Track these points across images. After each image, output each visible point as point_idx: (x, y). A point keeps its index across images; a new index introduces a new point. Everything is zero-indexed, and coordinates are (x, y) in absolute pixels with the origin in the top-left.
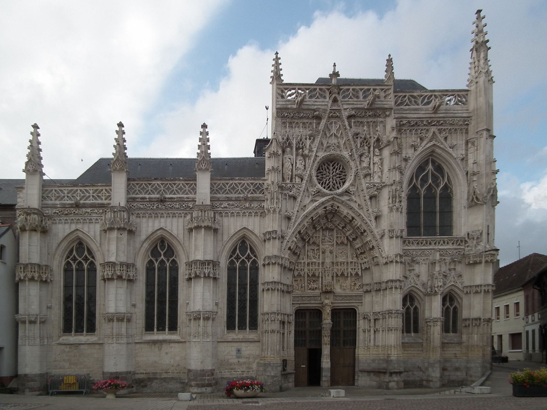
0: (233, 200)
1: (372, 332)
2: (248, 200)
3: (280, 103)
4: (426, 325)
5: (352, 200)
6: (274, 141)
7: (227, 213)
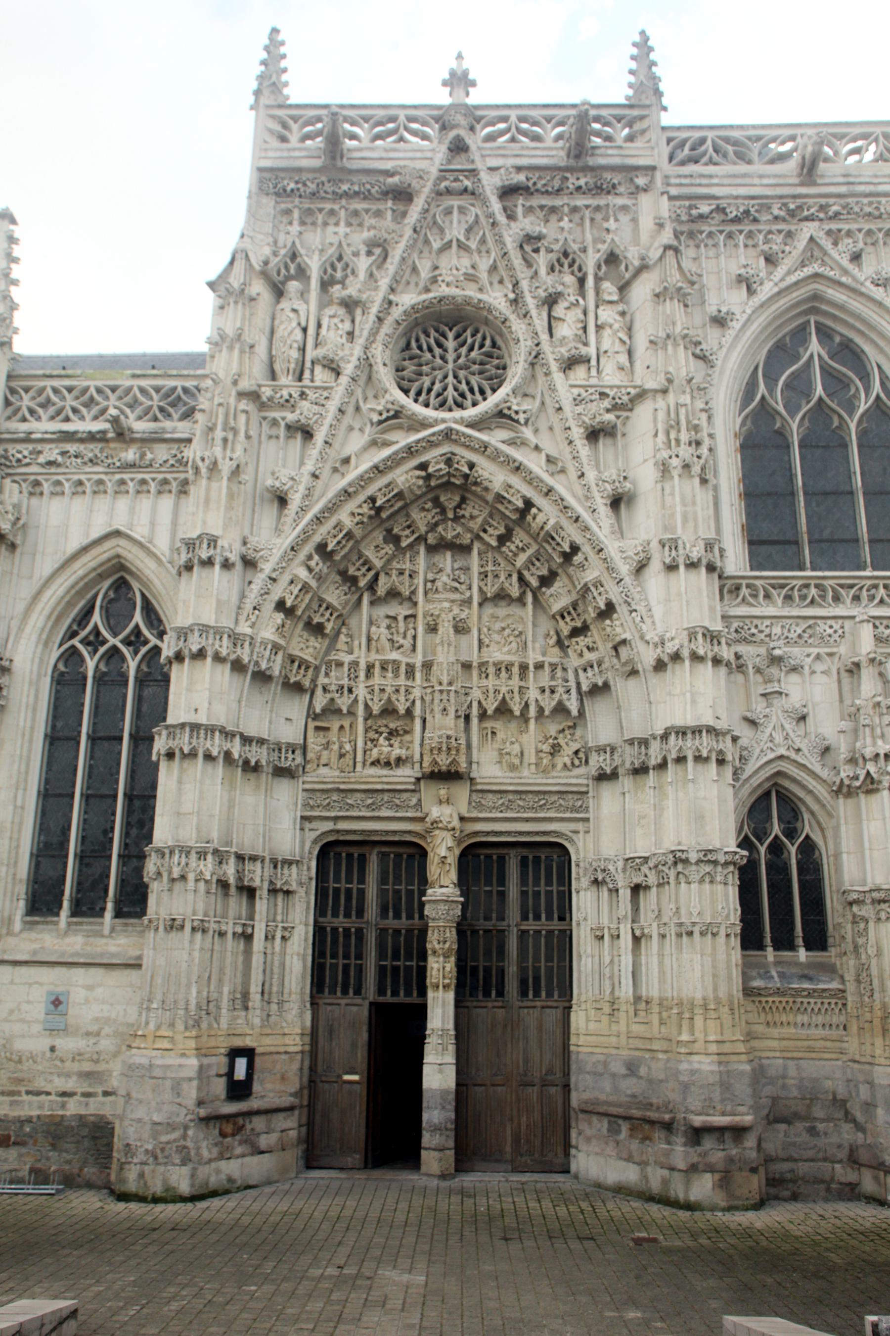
0: (82, 441)
1: (626, 940)
2: (133, 441)
3: (271, 154)
4: (850, 917)
5: (524, 443)
6: (238, 256)
7: (58, 483)
